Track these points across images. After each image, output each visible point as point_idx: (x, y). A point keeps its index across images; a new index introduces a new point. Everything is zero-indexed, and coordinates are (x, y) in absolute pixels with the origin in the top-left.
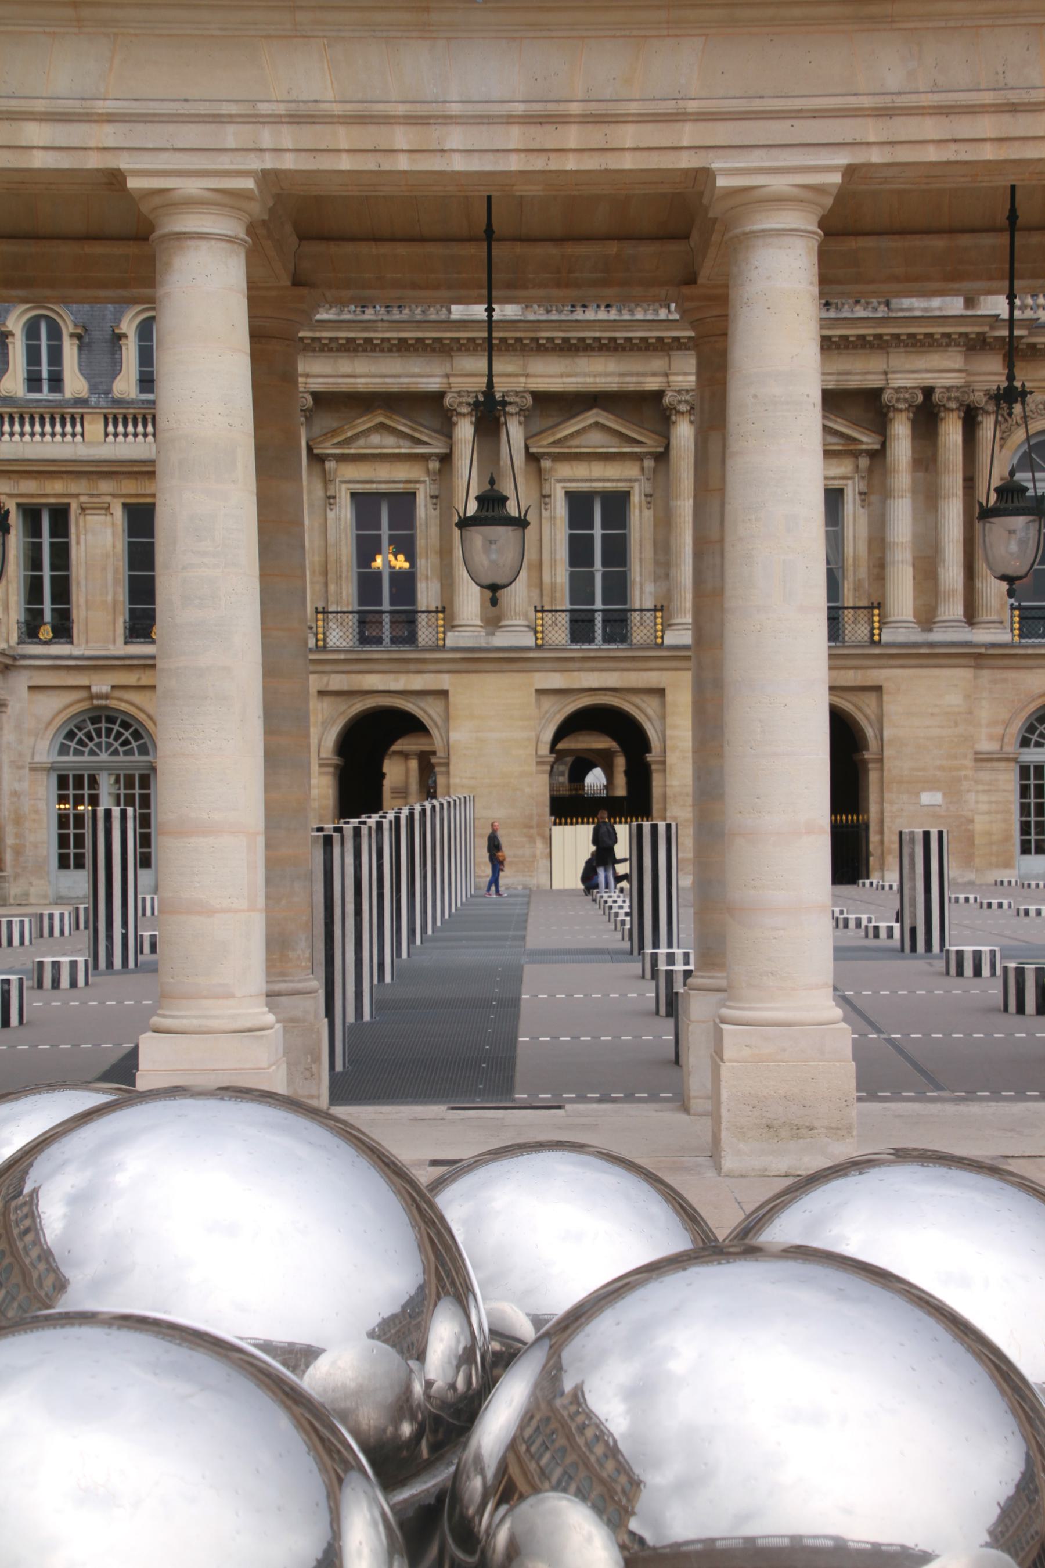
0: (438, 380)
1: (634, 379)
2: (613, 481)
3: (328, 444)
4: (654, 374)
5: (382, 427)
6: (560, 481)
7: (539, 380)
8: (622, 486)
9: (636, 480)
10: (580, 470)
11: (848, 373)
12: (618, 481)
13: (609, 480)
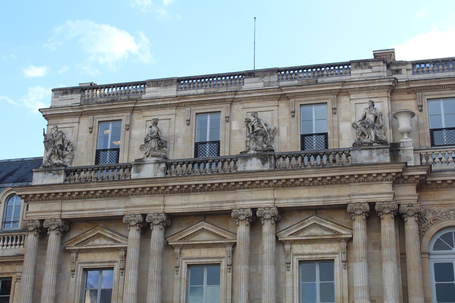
0: (122, 210)
1: (218, 205)
2: (211, 258)
3: (73, 245)
4: (228, 202)
5: (99, 236)
6: (184, 259)
7: (171, 207)
8: (216, 261)
9: (223, 257)
10: (195, 253)
11: (329, 197)
12: (214, 258)
13: (209, 258)
